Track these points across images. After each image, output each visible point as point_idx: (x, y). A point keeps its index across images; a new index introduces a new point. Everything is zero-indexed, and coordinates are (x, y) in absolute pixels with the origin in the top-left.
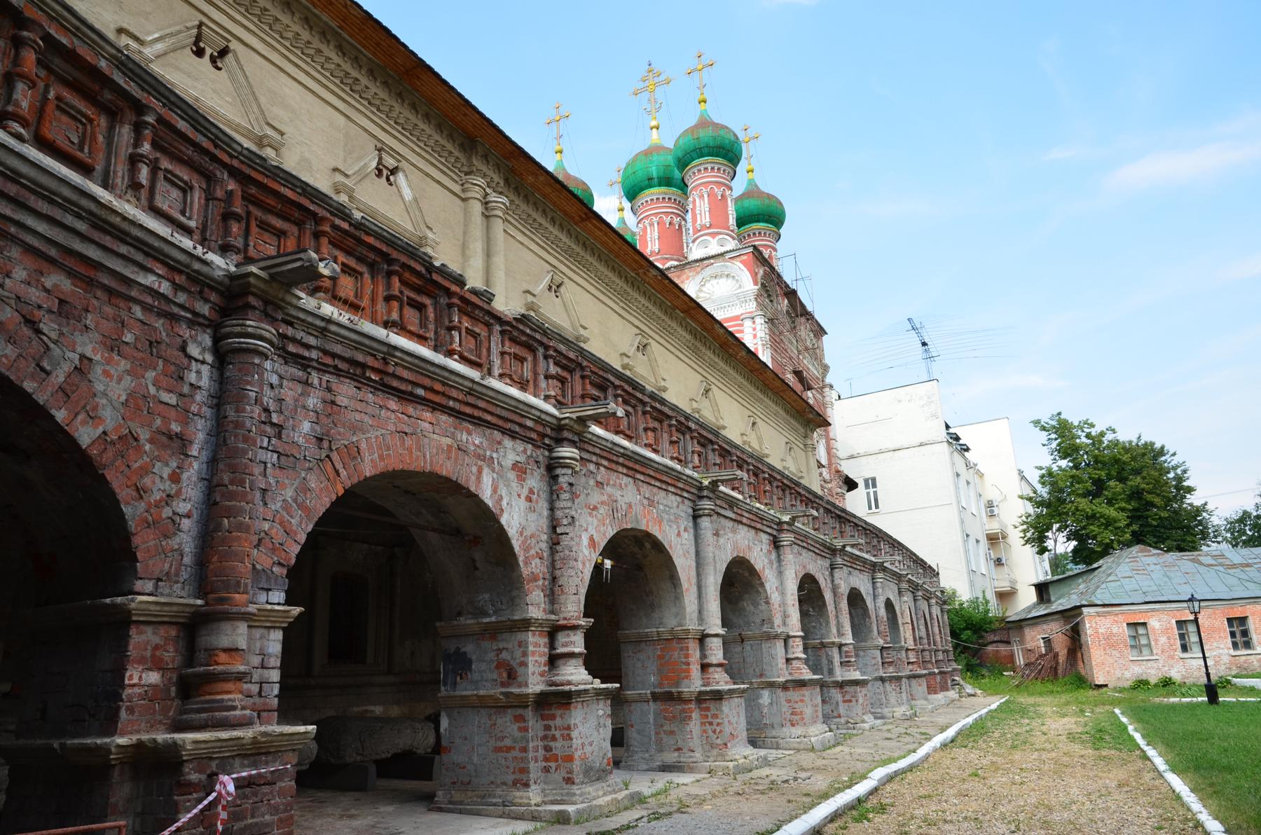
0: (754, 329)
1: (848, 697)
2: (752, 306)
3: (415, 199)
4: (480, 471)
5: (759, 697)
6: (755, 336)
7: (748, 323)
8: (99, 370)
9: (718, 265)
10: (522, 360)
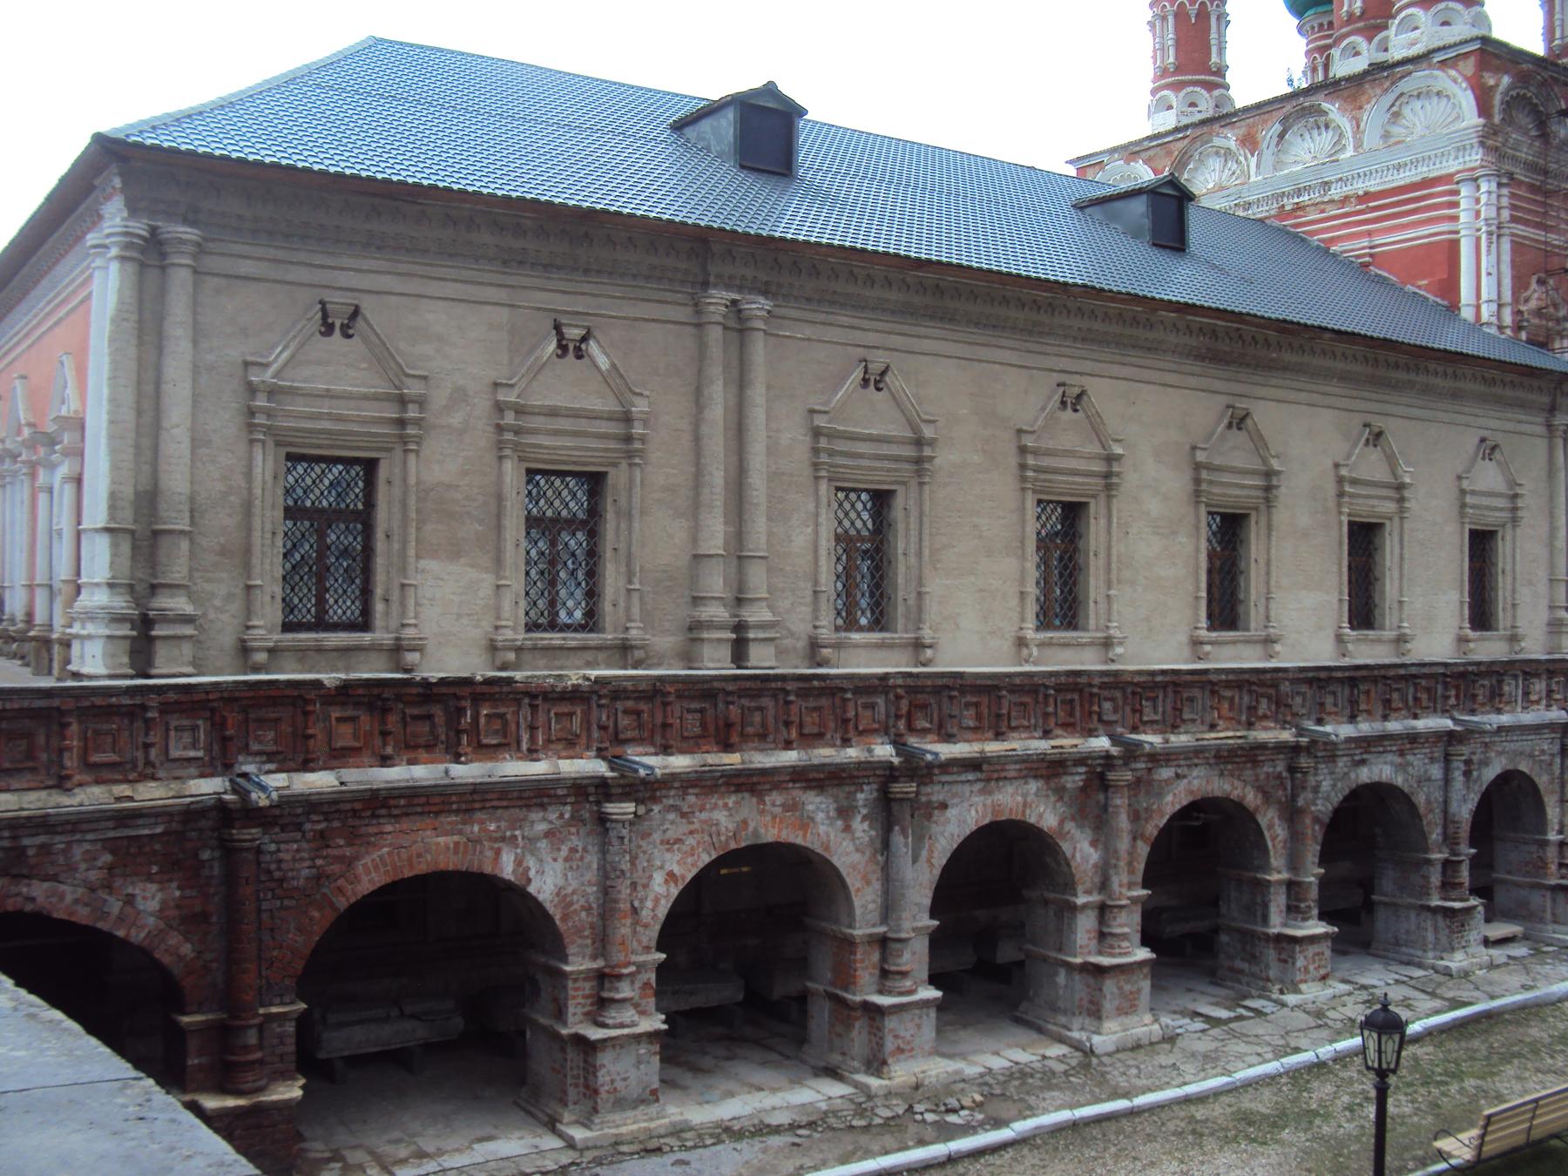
0: (1478, 201)
1: (1284, 956)
2: (1476, 157)
3: (613, 365)
4: (498, 852)
5: (1056, 974)
7: (1465, 191)
8: (139, 899)
9: (1419, 78)
10: (571, 715)
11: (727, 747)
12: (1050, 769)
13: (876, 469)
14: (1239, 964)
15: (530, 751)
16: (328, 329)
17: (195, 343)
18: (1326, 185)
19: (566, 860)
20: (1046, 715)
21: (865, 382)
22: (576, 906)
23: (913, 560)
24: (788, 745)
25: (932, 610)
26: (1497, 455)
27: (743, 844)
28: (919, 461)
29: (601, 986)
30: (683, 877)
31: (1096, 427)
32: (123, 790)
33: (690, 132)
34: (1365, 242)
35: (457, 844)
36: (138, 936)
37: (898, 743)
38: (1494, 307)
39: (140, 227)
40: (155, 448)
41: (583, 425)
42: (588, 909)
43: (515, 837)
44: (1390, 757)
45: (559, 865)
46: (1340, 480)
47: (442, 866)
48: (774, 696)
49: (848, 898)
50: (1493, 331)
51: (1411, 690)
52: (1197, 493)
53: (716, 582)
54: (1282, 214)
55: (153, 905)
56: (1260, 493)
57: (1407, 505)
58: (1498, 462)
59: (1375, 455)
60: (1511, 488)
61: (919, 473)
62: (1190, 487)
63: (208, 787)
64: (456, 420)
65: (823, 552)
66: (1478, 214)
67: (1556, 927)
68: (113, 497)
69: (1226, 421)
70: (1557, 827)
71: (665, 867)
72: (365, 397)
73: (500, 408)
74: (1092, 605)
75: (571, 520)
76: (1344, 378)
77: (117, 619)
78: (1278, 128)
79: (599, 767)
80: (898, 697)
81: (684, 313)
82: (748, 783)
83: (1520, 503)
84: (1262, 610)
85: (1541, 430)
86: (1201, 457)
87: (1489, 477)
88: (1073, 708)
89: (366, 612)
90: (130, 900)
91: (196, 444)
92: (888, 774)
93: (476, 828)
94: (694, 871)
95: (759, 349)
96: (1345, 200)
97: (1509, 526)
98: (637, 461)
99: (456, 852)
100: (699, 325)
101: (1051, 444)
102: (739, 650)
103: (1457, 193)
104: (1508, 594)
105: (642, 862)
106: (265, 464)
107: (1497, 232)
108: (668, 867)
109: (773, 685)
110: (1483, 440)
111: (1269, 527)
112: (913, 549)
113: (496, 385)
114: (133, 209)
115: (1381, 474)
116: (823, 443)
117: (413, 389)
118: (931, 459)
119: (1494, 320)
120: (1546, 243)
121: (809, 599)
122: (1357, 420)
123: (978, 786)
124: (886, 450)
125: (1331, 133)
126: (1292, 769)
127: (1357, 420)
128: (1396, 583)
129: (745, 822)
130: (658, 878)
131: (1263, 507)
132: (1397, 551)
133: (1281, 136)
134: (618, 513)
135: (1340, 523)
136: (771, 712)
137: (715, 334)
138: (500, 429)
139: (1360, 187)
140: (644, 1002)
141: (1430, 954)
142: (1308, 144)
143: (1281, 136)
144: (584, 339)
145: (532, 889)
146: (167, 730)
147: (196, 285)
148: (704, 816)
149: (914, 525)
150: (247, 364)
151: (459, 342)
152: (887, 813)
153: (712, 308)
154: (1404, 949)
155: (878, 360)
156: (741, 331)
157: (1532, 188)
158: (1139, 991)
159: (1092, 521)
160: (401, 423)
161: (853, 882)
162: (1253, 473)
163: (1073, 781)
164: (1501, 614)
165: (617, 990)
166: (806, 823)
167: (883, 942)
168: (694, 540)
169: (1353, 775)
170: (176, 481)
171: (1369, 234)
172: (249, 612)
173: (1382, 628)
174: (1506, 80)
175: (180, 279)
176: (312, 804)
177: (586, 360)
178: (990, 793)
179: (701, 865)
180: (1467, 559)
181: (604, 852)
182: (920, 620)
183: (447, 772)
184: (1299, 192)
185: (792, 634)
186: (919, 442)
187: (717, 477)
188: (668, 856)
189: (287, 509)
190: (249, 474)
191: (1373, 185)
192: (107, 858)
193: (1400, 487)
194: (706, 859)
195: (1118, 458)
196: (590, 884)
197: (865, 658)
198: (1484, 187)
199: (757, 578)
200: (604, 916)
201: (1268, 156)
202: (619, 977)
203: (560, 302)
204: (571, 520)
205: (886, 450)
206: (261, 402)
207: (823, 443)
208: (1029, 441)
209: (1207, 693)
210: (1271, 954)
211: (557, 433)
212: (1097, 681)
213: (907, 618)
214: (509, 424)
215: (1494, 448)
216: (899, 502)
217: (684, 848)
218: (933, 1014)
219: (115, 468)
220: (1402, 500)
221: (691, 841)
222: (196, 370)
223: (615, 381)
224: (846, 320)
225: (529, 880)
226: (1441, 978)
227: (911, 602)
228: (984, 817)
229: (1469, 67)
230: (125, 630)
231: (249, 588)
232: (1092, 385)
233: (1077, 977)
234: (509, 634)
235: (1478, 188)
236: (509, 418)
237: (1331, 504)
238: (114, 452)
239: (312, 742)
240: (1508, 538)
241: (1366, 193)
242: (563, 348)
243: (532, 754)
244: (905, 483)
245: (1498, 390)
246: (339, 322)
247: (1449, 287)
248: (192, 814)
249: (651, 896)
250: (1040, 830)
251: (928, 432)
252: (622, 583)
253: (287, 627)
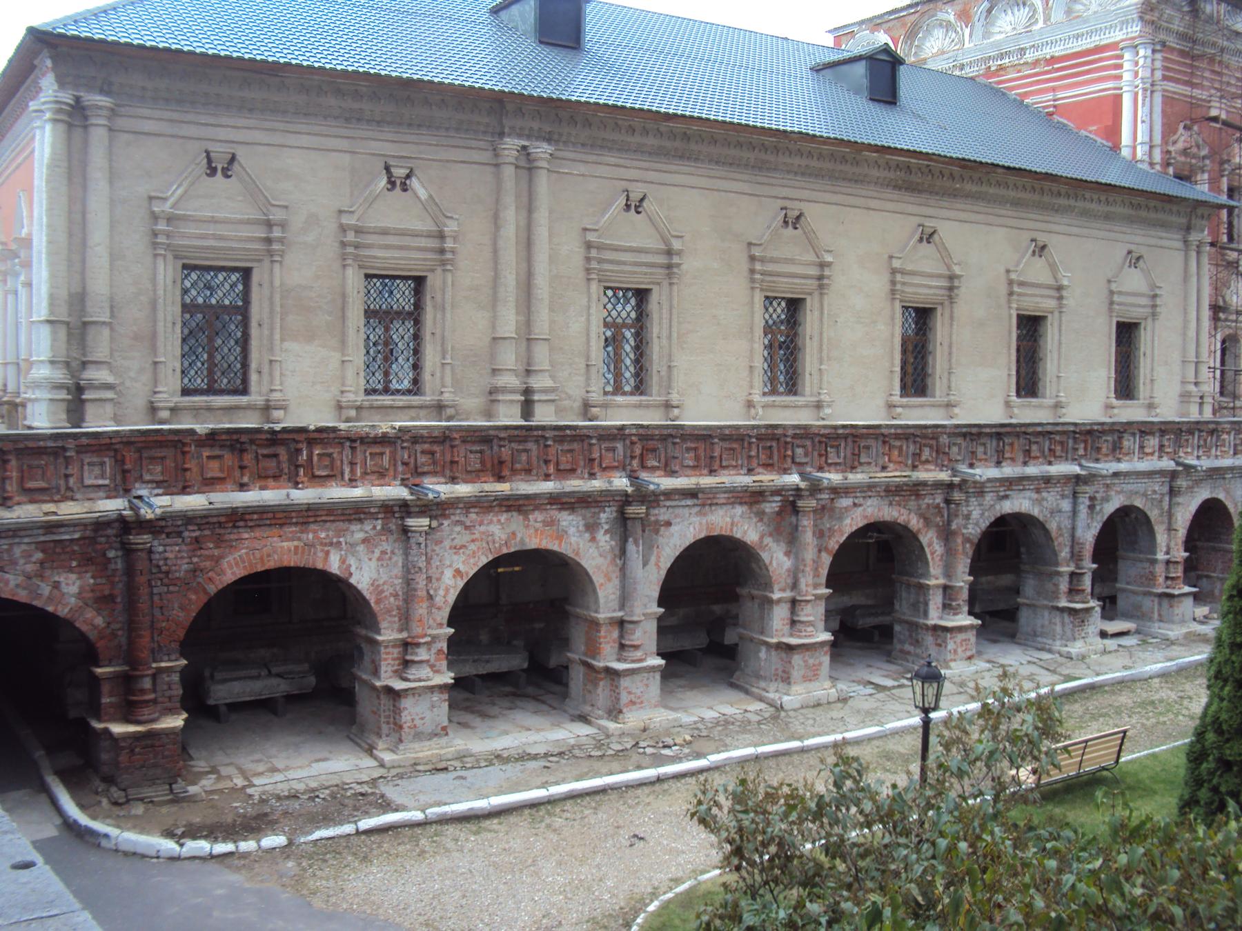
0: (1136, 64)
1: (939, 641)
2: (1136, 29)
3: (431, 196)
4: (327, 553)
5: (759, 651)
6: (1136, 74)
7: (1127, 55)
8: (63, 585)
10: (382, 454)
11: (500, 478)
12: (753, 497)
13: (635, 273)
14: (907, 647)
15: (350, 480)
16: (212, 171)
17: (111, 183)
18: (1022, 51)
19: (379, 559)
20: (750, 457)
21: (628, 206)
22: (387, 593)
23: (665, 342)
24: (547, 477)
25: (679, 380)
26: (1141, 263)
27: (513, 550)
28: (669, 267)
29: (406, 652)
30: (467, 574)
31: (811, 242)
32: (50, 507)
33: (504, 15)
34: (1050, 96)
35: (296, 548)
36: (63, 612)
37: (633, 477)
38: (1146, 148)
39: (67, 97)
40: (84, 261)
41: (407, 241)
42: (396, 595)
43: (339, 543)
44: (1028, 494)
45: (374, 564)
46: (1011, 283)
47: (285, 564)
48: (537, 441)
49: (594, 590)
50: (1145, 166)
51: (1047, 443)
52: (893, 292)
53: (509, 357)
54: (989, 73)
55: (74, 589)
56: (946, 292)
57: (1065, 302)
58: (1142, 270)
59: (1040, 263)
60: (1152, 290)
61: (670, 276)
62: (888, 287)
63: (113, 506)
64: (310, 238)
65: (593, 335)
66: (1136, 74)
67: (1162, 624)
68: (52, 299)
69: (917, 237)
70: (1164, 549)
71: (454, 563)
72: (241, 222)
73: (343, 229)
74: (807, 376)
75: (398, 310)
76: (1016, 203)
77: (58, 387)
79: (403, 493)
80: (633, 443)
81: (486, 156)
82: (516, 505)
83: (1158, 302)
84: (945, 381)
85: (1180, 245)
86: (896, 264)
87: (1134, 281)
88: (772, 453)
89: (245, 380)
90: (56, 586)
91: (114, 257)
92: (625, 500)
93: (311, 536)
94: (476, 569)
95: (543, 182)
96: (1036, 63)
97: (1150, 320)
98: (449, 267)
99: (296, 553)
100: (497, 165)
101: (775, 254)
102: (527, 408)
103: (1121, 57)
104: (1148, 371)
105: (435, 562)
106: (167, 272)
107: (1151, 89)
108: (455, 566)
109: (535, 433)
110: (1129, 252)
111: (952, 318)
112: (665, 333)
113: (341, 212)
114: (62, 82)
115: (1045, 277)
116: (594, 253)
117: (277, 215)
118: (678, 265)
119: (1146, 158)
120: (1191, 97)
121: (583, 371)
122: (1027, 236)
123: (696, 509)
125: (1027, 9)
126: (948, 502)
127: (1027, 236)
128: (1056, 362)
129: (514, 534)
130: (448, 573)
131: (947, 303)
132: (1056, 338)
133: (989, 11)
134: (434, 307)
135: (1010, 316)
136: (534, 453)
137: (508, 172)
138: (343, 244)
139: (1048, 52)
140: (438, 664)
141: (1058, 643)
142: (1009, 17)
143: (989, 11)
144: (408, 176)
145: (353, 581)
146: (82, 465)
147: (111, 140)
148: (483, 528)
149: (665, 315)
150: (151, 198)
151: (312, 181)
152: (624, 526)
153: (506, 152)
154: (1039, 639)
155: (637, 191)
156: (530, 169)
157: (1182, 53)
158: (820, 664)
159: (808, 312)
160: (269, 241)
161: (598, 579)
162: (939, 276)
163: (771, 506)
164: (1141, 387)
165: (416, 654)
166: (561, 536)
167: (621, 623)
168: (494, 327)
169: (998, 507)
170: (99, 285)
171: (1054, 89)
172: (156, 382)
173: (1044, 397)
175: (98, 135)
176: (188, 519)
177: (409, 192)
178: (705, 515)
179: (481, 565)
180: (1114, 345)
181: (406, 554)
182: (669, 387)
183: (288, 495)
184: (1002, 56)
185: (570, 397)
186: (669, 253)
187: (510, 279)
188: (455, 557)
189: (184, 306)
190: (154, 280)
191: (1058, 51)
192: (39, 555)
193: (1059, 288)
194: (484, 560)
195: (829, 264)
196: (396, 577)
197: (625, 413)
198: (1142, 52)
199: (541, 355)
200: (406, 601)
201: (979, 27)
202: (418, 645)
203: (390, 149)
204: (398, 310)
206: (162, 226)
207: (594, 253)
208: (757, 252)
209: (880, 443)
210: (929, 639)
211: (387, 247)
212: (790, 432)
213: (660, 386)
214: (352, 238)
215: (1138, 259)
216: (654, 298)
217: (468, 552)
218: (658, 676)
219: (53, 276)
220: (1060, 298)
221: (473, 547)
222: (112, 202)
223: (433, 208)
224: (613, 160)
225: (351, 574)
226: (1064, 660)
227: (663, 373)
228: (700, 531)
230: (63, 395)
231: (156, 363)
232: (806, 207)
233: (773, 653)
234: (351, 397)
235: (1137, 53)
236: (351, 237)
237: (1003, 300)
238: (52, 264)
239: (188, 473)
240: (1149, 328)
241: (1052, 57)
242: (392, 183)
243: (352, 482)
244: (659, 284)
245: (1143, 213)
246: (219, 166)
247: (1113, 132)
248: (100, 525)
249: (443, 587)
250: (745, 543)
251: (676, 245)
252: (438, 359)
253: (186, 392)
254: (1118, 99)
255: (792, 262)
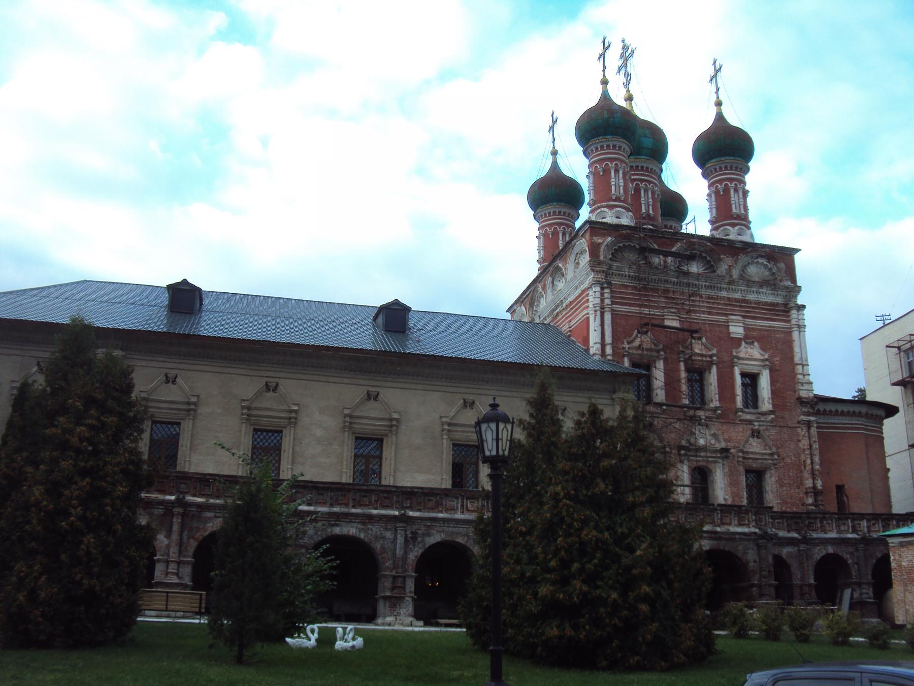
21: (167, 381)
38: (599, 346)
44: (355, 525)
78: (550, 279)
101: (259, 405)
120: (640, 313)
124: (174, 406)
133: (553, 282)
143: (553, 282)
155: (172, 373)
157: (635, 288)
169: (329, 530)
174: (609, 239)
184: (557, 307)
191: (571, 299)
205: (174, 406)
229: (587, 235)
247: (586, 340)
254: (588, 318)
255: (271, 408)
